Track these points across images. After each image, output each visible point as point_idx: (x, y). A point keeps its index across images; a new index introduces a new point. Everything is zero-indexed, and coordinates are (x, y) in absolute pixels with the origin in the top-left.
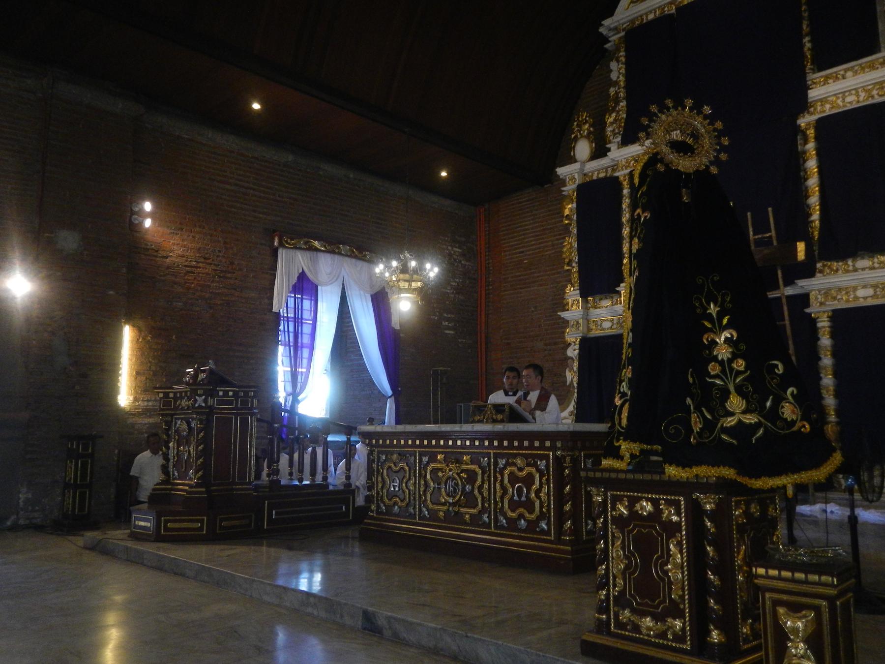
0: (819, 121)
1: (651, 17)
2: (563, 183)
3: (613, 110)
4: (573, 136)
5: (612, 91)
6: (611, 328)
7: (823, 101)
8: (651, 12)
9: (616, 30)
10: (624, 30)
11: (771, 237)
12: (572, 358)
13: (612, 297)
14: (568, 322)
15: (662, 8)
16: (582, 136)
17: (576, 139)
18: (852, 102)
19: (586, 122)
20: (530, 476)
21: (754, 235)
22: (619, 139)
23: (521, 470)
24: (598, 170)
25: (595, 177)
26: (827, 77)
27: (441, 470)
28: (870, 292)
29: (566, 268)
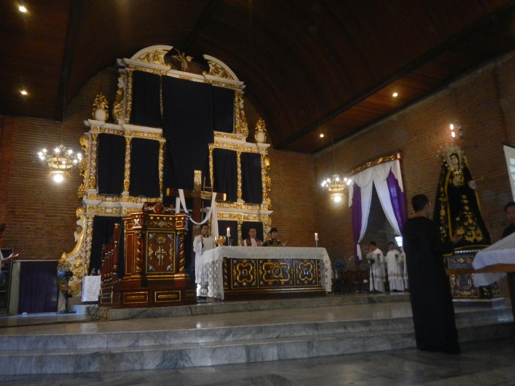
0: (215, 149)
1: (148, 71)
2: (88, 129)
3: (119, 102)
4: (94, 105)
5: (119, 92)
6: (111, 213)
7: (217, 143)
8: (148, 68)
9: (128, 66)
10: (132, 68)
11: (211, 189)
12: (79, 226)
13: (113, 197)
15: (154, 70)
16: (100, 108)
18: (225, 147)
19: (104, 101)
20: (309, 266)
21: (206, 186)
22: (128, 119)
23: (306, 263)
24: (109, 129)
25: (106, 132)
26: (219, 134)
27: (272, 265)
28: (227, 216)
29: (81, 174)
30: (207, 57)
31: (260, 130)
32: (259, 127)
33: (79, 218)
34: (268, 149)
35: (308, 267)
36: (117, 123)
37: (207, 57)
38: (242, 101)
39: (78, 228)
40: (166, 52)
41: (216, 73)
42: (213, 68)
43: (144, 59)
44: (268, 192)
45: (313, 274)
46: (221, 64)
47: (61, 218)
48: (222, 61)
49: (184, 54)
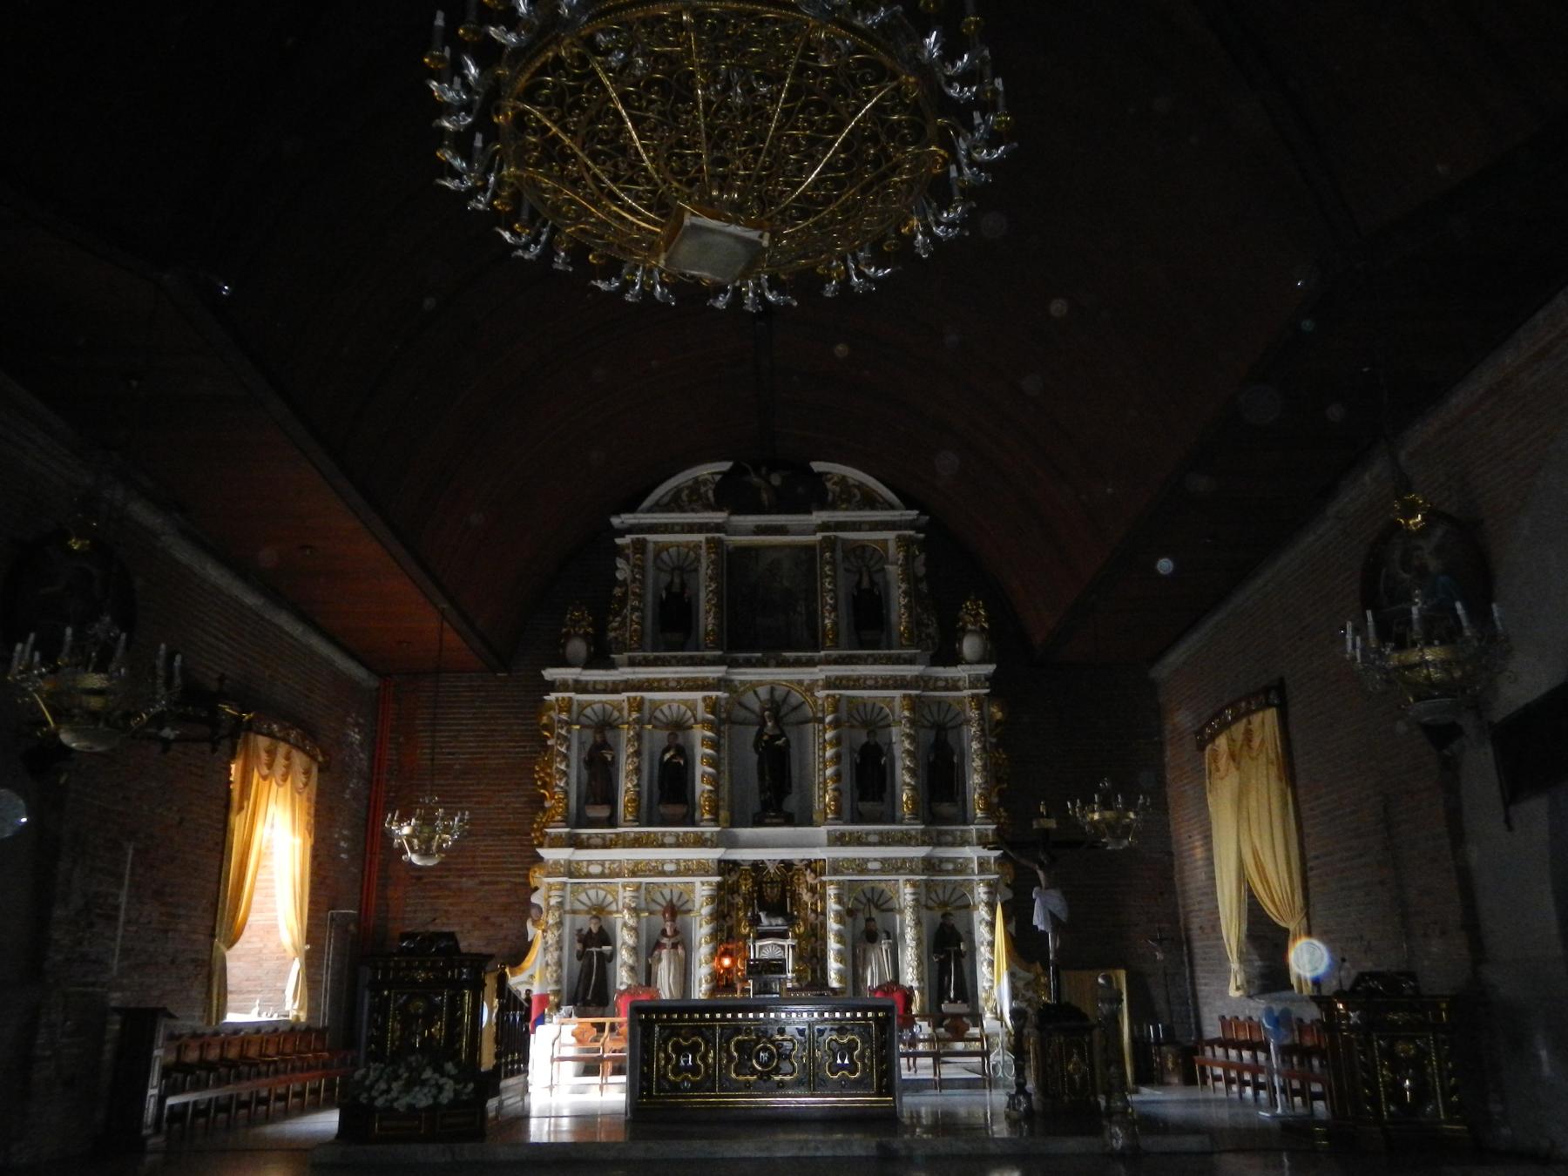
3: (617, 614)
14: (541, 859)
16: (576, 635)
17: (568, 636)
30: (818, 466)
31: (969, 627)
32: (967, 618)
33: (536, 889)
34: (992, 680)
35: (851, 1047)
36: (612, 665)
37: (818, 466)
38: (923, 556)
39: (534, 912)
40: (718, 478)
41: (843, 501)
42: (838, 489)
43: (667, 505)
44: (1001, 793)
45: (864, 1064)
46: (855, 474)
47: (507, 886)
48: (854, 466)
49: (764, 470)
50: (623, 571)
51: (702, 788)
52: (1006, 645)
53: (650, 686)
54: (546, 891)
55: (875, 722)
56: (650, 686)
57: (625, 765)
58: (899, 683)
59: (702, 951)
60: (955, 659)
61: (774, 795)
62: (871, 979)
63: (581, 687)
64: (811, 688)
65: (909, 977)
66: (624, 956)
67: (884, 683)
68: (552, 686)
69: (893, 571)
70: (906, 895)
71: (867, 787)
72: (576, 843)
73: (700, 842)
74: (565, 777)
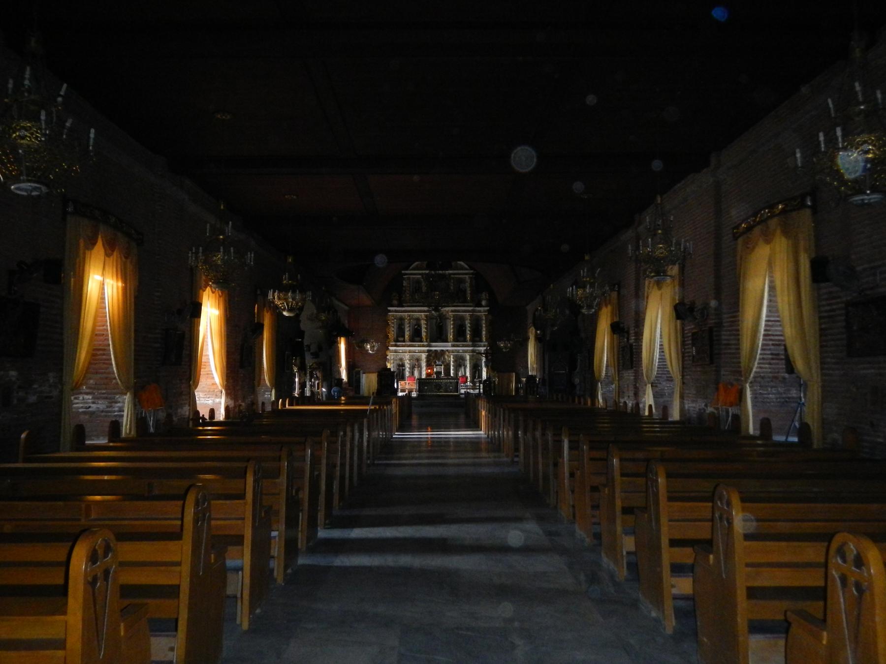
50: (405, 283)
51: (424, 334)
52: (493, 304)
53: (413, 311)
54: (390, 356)
55: (462, 319)
56: (413, 311)
57: (407, 329)
58: (468, 311)
59: (424, 369)
60: (481, 306)
61: (439, 335)
62: (460, 374)
63: (396, 311)
64: (448, 312)
65: (468, 374)
66: (407, 370)
67: (465, 311)
68: (390, 311)
69: (468, 284)
70: (468, 357)
71: (460, 336)
72: (396, 346)
73: (423, 346)
74: (392, 333)
